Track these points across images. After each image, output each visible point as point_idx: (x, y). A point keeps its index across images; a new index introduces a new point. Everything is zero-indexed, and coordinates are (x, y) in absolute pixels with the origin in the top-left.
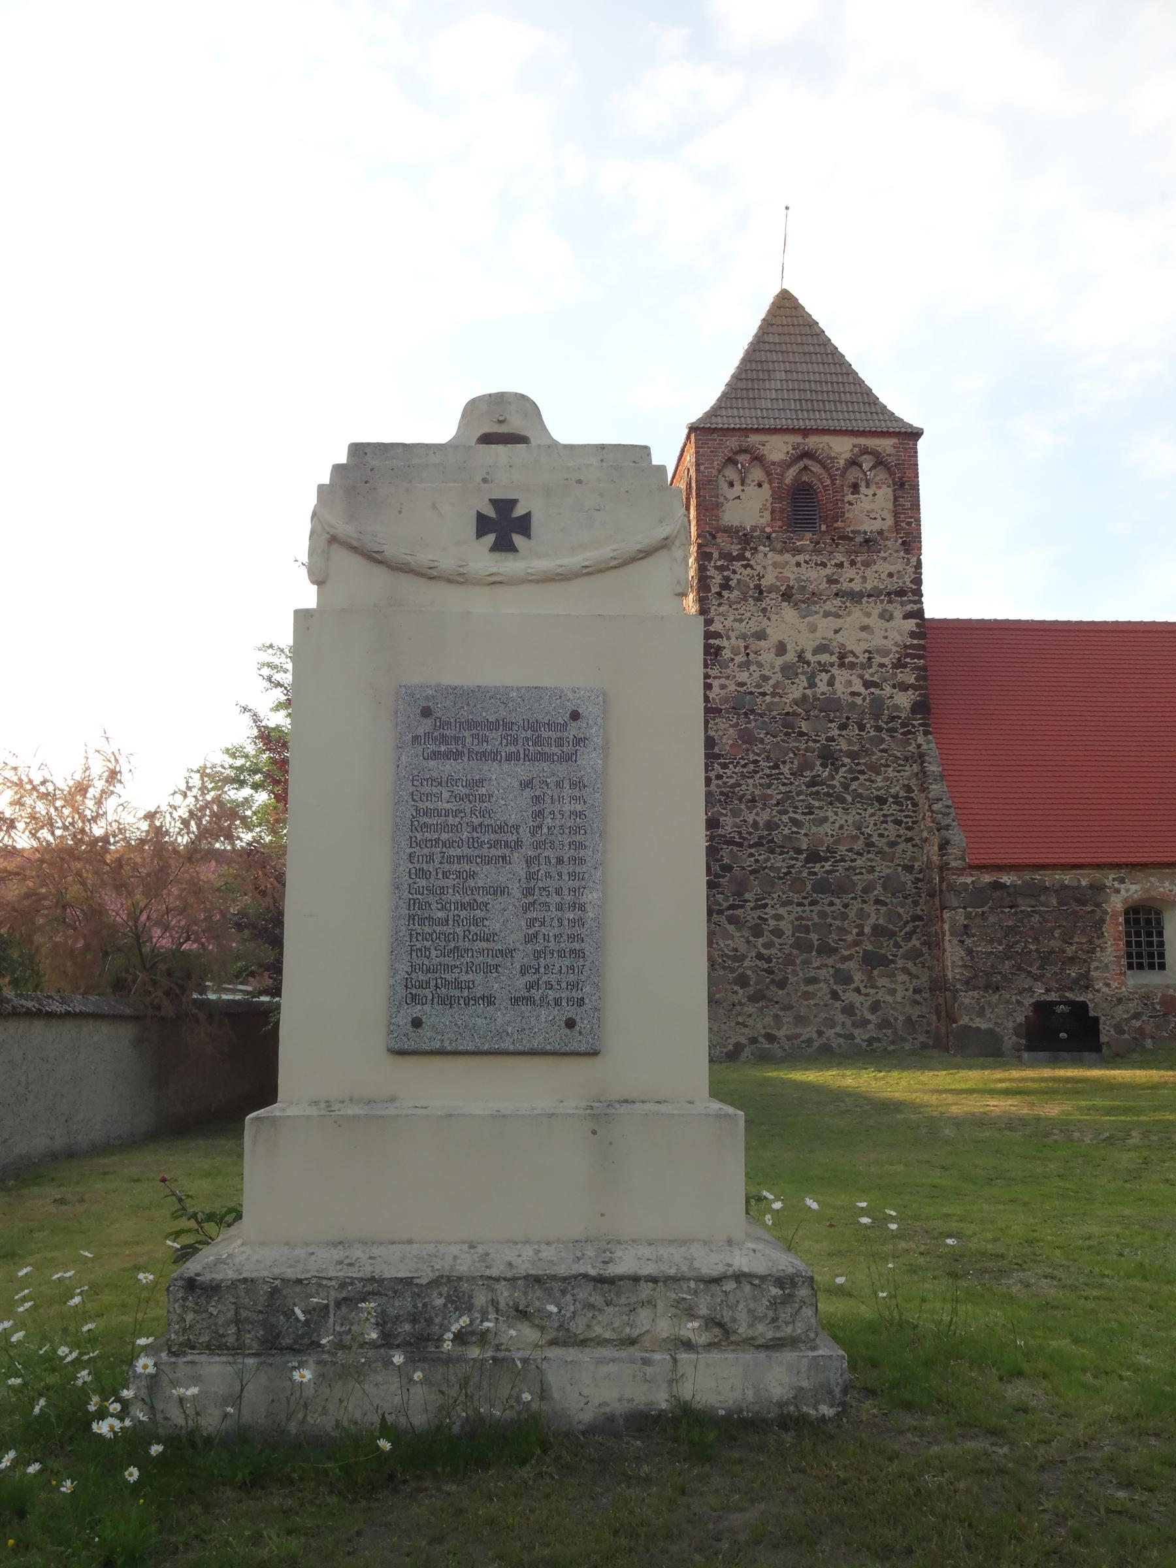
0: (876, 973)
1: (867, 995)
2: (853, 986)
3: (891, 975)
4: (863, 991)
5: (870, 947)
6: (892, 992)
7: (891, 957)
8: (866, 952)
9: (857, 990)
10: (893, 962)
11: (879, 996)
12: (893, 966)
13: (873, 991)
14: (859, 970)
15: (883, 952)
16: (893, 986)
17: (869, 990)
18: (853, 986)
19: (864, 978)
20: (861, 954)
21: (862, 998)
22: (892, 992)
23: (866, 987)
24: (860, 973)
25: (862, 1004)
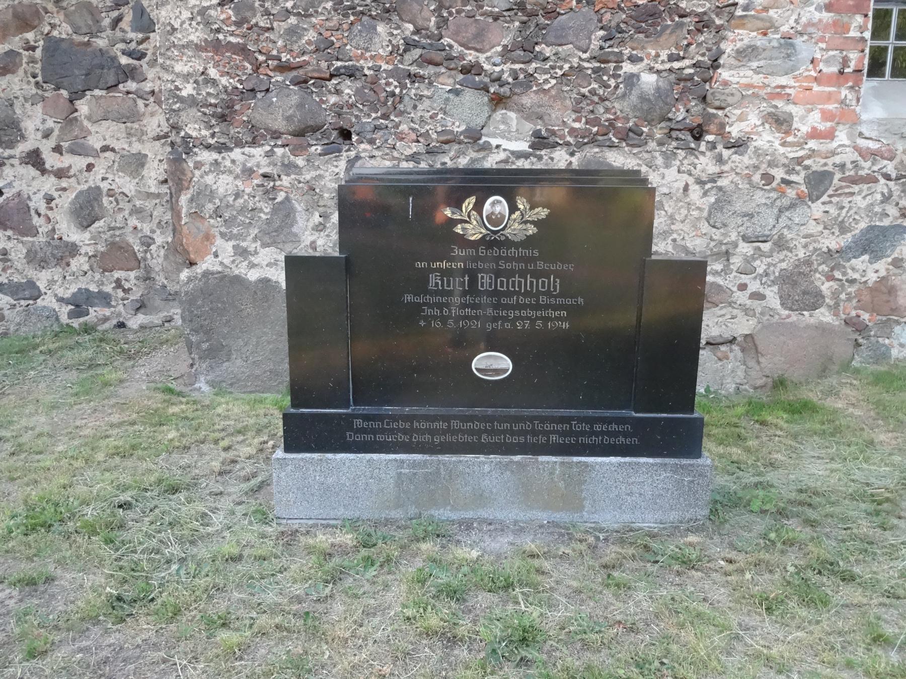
0: (83, 107)
1: (61, 174)
2: (23, 148)
3: (129, 117)
4: (52, 161)
5: (64, 31)
6: (136, 164)
7: (124, 60)
8: (53, 46)
9: (34, 159)
10: (130, 73)
11: (94, 179)
12: (132, 85)
13: (80, 162)
14: (34, 100)
15: (101, 43)
16: (136, 147)
17: (67, 160)
18: (23, 148)
19: (50, 123)
20: (38, 53)
21: (49, 184)
22: (136, 164)
23: (58, 149)
24: (39, 108)
25: (49, 199)
